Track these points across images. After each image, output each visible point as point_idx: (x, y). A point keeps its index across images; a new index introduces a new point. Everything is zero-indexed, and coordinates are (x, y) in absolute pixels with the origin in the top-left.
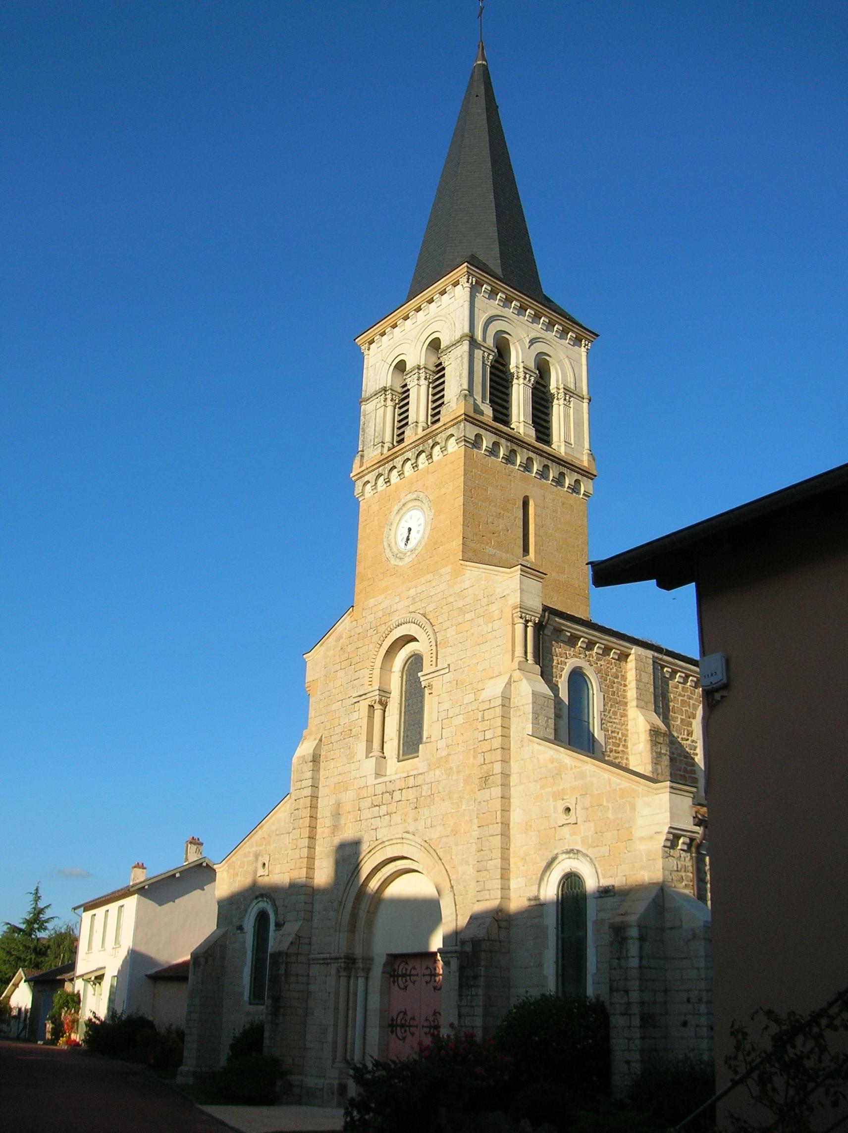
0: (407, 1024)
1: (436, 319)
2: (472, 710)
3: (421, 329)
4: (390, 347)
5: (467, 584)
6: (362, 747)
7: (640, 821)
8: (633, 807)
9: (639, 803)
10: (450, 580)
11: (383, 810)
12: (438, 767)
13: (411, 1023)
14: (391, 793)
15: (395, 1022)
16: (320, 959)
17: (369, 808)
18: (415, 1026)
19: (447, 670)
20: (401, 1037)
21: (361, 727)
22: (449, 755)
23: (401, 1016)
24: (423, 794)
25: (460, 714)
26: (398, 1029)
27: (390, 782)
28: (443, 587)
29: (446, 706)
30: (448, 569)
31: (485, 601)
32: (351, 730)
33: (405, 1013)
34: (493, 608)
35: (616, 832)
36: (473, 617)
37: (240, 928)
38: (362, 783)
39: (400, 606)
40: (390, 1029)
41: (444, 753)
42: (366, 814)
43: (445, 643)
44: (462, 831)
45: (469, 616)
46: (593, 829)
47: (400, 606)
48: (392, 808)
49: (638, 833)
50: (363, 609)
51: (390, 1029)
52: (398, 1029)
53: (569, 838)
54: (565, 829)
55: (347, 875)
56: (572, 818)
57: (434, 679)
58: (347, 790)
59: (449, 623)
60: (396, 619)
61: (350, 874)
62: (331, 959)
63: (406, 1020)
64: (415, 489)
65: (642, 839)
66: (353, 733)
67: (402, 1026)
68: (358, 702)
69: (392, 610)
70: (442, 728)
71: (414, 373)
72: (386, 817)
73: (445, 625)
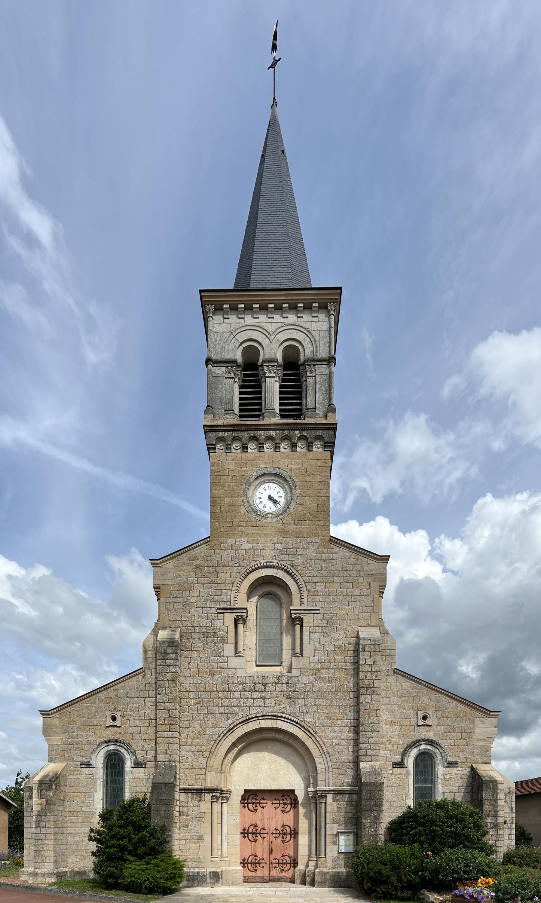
0: (258, 832)
1: (296, 327)
2: (342, 643)
3: (279, 328)
4: (241, 325)
5: (335, 556)
6: (229, 649)
7: (477, 730)
8: (473, 722)
9: (477, 720)
10: (318, 548)
11: (256, 695)
12: (312, 675)
13: (262, 831)
14: (265, 685)
15: (246, 831)
16: (193, 790)
17: (241, 692)
18: (265, 833)
19: (319, 612)
20: (252, 840)
21: (227, 633)
22: (322, 668)
23: (252, 827)
24: (297, 690)
25: (332, 644)
26: (250, 836)
27: (263, 677)
28: (311, 551)
29: (317, 635)
30: (316, 539)
31: (353, 573)
32: (215, 633)
33: (256, 825)
34: (360, 579)
35: (460, 734)
36: (342, 580)
37: (88, 765)
38: (230, 673)
39: (264, 552)
40: (243, 835)
41: (318, 667)
42: (237, 695)
43: (314, 592)
44: (336, 718)
45: (337, 579)
46: (442, 730)
47: (264, 552)
48: (264, 694)
49: (476, 736)
50: (221, 543)
51: (243, 835)
52: (250, 836)
53: (424, 733)
54: (422, 728)
55: (219, 735)
56: (428, 722)
57: (305, 614)
58: (214, 675)
59: (318, 579)
60: (261, 561)
61: (222, 735)
62: (205, 790)
63: (257, 830)
64: (278, 466)
65: (479, 740)
66: (219, 634)
67: (253, 833)
68: (223, 613)
69: (256, 554)
70: (315, 650)
71: (273, 364)
72: (259, 700)
73: (314, 579)
